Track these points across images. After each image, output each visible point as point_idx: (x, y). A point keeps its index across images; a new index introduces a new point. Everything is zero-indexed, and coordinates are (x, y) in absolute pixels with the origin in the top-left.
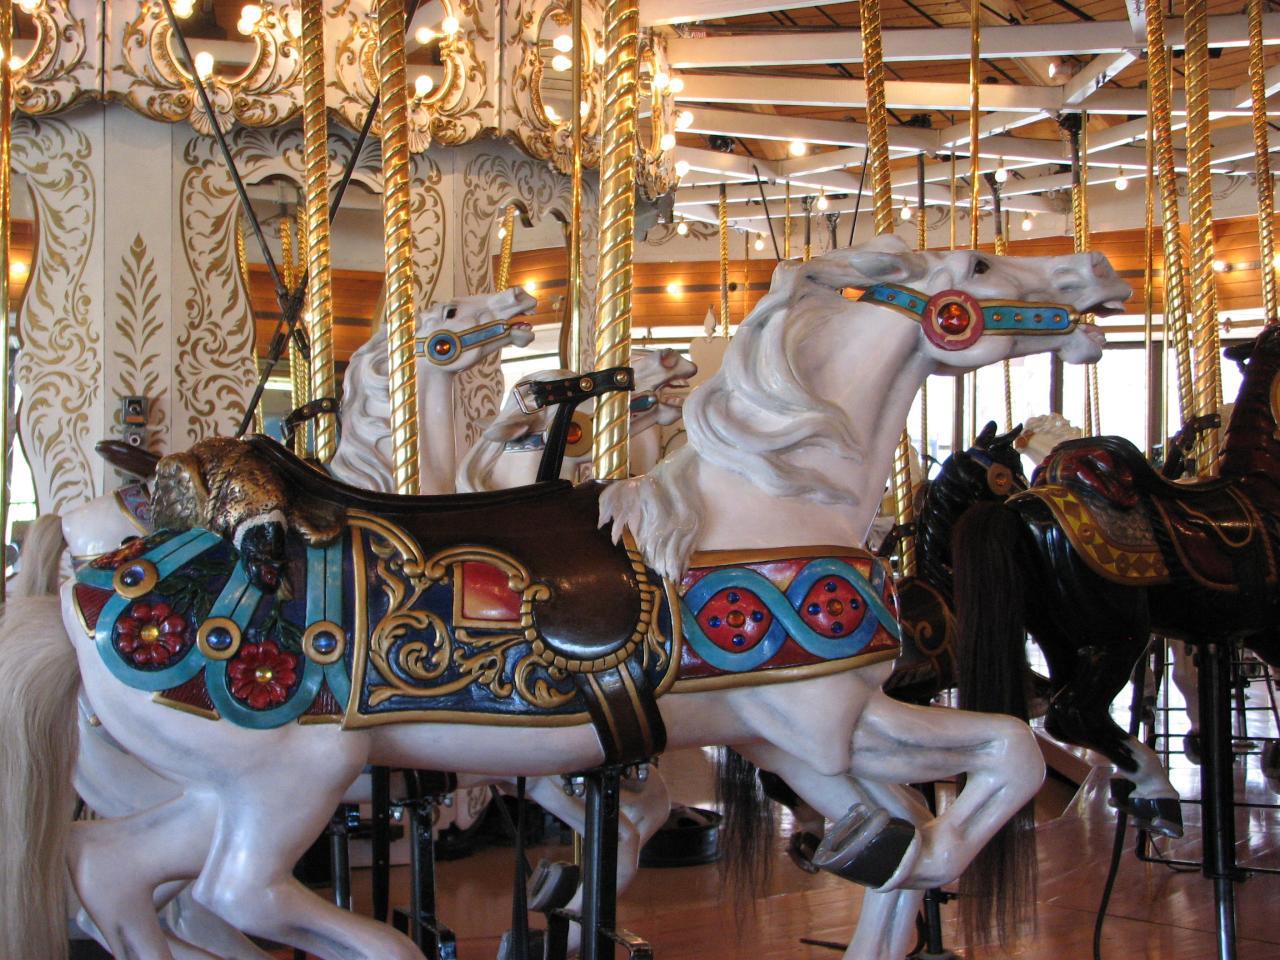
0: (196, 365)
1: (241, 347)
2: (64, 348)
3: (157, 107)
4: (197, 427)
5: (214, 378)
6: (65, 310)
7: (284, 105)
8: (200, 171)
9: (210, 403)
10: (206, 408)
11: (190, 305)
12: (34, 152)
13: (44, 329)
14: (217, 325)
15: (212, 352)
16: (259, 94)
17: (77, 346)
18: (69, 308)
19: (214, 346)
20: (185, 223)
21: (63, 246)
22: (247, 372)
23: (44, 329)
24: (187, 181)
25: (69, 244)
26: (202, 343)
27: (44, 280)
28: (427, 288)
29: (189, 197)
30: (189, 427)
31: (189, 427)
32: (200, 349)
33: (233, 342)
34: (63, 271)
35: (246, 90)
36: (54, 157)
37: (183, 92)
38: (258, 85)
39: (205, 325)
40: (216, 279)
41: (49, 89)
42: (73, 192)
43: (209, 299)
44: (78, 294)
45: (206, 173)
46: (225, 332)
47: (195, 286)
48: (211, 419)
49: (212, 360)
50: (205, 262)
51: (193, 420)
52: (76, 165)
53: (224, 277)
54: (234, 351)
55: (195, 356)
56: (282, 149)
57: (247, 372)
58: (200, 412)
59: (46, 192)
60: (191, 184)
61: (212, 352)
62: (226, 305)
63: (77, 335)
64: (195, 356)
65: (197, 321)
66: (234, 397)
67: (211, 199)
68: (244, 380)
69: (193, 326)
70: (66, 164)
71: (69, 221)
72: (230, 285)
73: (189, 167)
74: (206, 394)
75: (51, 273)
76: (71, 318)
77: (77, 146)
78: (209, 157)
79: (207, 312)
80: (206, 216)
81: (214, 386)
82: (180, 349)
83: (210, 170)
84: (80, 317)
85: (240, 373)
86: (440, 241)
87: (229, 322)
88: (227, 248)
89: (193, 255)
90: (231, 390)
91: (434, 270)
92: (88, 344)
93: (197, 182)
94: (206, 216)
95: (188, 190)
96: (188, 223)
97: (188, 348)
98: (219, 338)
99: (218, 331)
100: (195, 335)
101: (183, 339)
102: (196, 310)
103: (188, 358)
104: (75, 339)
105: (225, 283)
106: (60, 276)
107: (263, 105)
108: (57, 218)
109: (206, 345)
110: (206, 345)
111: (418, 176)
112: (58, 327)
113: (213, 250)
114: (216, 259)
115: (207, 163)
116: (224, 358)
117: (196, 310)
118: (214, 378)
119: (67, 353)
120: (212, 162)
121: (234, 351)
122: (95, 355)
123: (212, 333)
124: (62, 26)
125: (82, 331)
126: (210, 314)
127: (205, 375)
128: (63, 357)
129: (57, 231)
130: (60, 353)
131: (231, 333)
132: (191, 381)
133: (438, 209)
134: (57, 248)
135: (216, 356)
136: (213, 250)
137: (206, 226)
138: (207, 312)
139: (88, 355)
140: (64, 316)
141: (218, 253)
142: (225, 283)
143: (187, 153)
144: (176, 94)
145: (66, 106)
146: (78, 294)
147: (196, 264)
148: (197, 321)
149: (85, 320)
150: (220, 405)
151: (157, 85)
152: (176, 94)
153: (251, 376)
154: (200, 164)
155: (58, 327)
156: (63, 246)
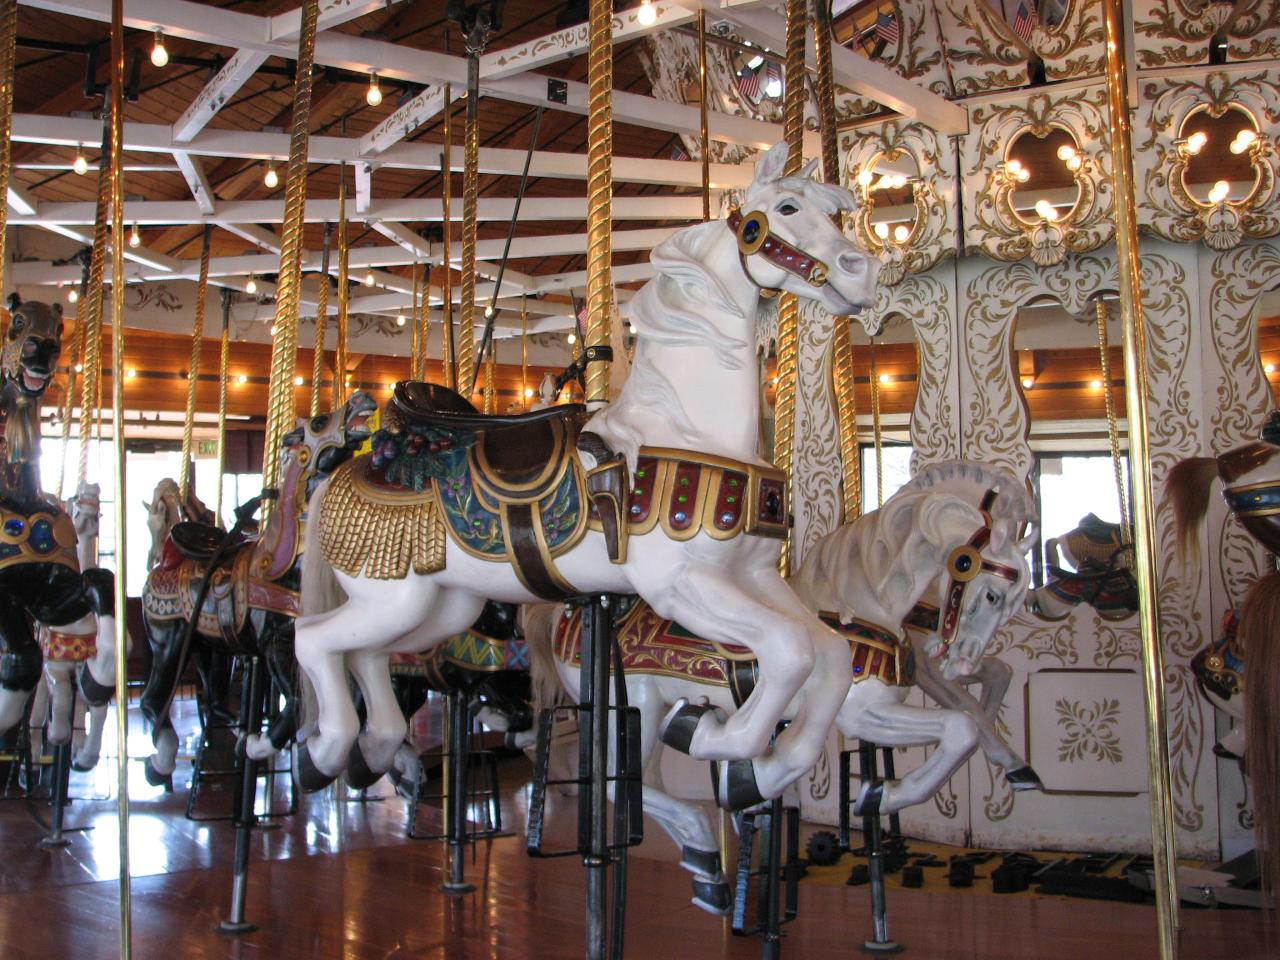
0: (1227, 438)
1: (1013, 436)
2: (1168, 434)
3: (1176, 231)
4: (808, 509)
5: (818, 474)
6: (1169, 403)
7: (1104, 229)
8: (1224, 282)
9: (816, 491)
10: (813, 495)
11: (1221, 390)
12: (916, 303)
13: (924, 432)
14: (818, 436)
15: (816, 455)
16: (1082, 227)
17: (1179, 432)
18: (1172, 401)
19: (993, 437)
20: (1215, 326)
21: (934, 369)
22: (835, 467)
23: (924, 432)
24: (1215, 291)
25: (1169, 351)
26: (983, 435)
27: (1152, 382)
28: (1175, 372)
29: (1217, 304)
30: (804, 509)
31: (804, 509)
32: (982, 439)
33: (828, 446)
34: (934, 387)
35: (1251, 209)
36: (1154, 285)
37: (1197, 217)
38: (1259, 204)
39: (812, 437)
40: (1241, 369)
41: (925, 252)
42: (1172, 310)
43: (1236, 386)
44: (1179, 390)
45: (1229, 284)
46: (1001, 426)
47: (1224, 375)
48: (815, 503)
49: (993, 448)
50: (1232, 355)
51: (807, 504)
52: (1173, 289)
53: (1248, 367)
54: (1009, 439)
55: (979, 446)
56: (1045, 276)
57: (835, 467)
58: (810, 498)
59: (924, 330)
60: (972, 315)
61: (992, 441)
62: (1251, 389)
63: (1179, 423)
64: (979, 446)
65: (979, 419)
66: (828, 487)
67: (1236, 305)
68: (1018, 461)
69: (1223, 408)
70: (1164, 288)
71: (1169, 333)
72: (1005, 389)
73: (1216, 280)
74: (813, 485)
75: (1156, 374)
76: (1174, 409)
77: (941, 295)
78: (986, 292)
79: (1235, 395)
80: (1231, 319)
81: (817, 479)
82: (1215, 427)
83: (1232, 281)
84: (1181, 409)
85: (1014, 456)
86: (1187, 330)
87: (825, 434)
88: (1002, 362)
89: (1222, 351)
90: (827, 482)
91: (945, 371)
92: (1189, 430)
93: (1223, 292)
94: (1231, 319)
95: (970, 319)
96: (1216, 324)
97: (1220, 425)
98: (997, 429)
99: (996, 425)
100: (807, 444)
101: (1216, 418)
102: (1225, 395)
103: (803, 461)
104: (1177, 426)
105: (1248, 372)
106: (1163, 376)
107: (1087, 234)
108: (929, 347)
109: (1236, 422)
110: (1236, 422)
111: (1163, 278)
112: (1163, 418)
113: (1237, 346)
114: (1240, 353)
115: (1230, 276)
116: (823, 459)
117: (1225, 395)
118: (818, 474)
119: (1171, 438)
120: (988, 296)
121: (828, 454)
122: (1195, 437)
123: (992, 426)
124: (1097, 182)
125: (1183, 419)
126: (990, 411)
127: (813, 471)
128: (1168, 441)
129: (1161, 342)
130: (1166, 438)
131: (827, 441)
132: (805, 476)
133: (1184, 304)
134: (931, 371)
135: (995, 444)
136: (1237, 346)
137: (1232, 327)
138: (1235, 395)
139: (950, 449)
140: (1168, 408)
141: (995, 365)
142: (1248, 372)
143: (1214, 269)
144: (1017, 239)
145: (1105, 243)
146: (1179, 390)
147: (977, 374)
148: (979, 419)
149: (1186, 411)
150: (821, 492)
151: (1005, 235)
152: (1017, 239)
153: (1023, 458)
154: (1224, 278)
155: (1163, 418)
156: (934, 369)
